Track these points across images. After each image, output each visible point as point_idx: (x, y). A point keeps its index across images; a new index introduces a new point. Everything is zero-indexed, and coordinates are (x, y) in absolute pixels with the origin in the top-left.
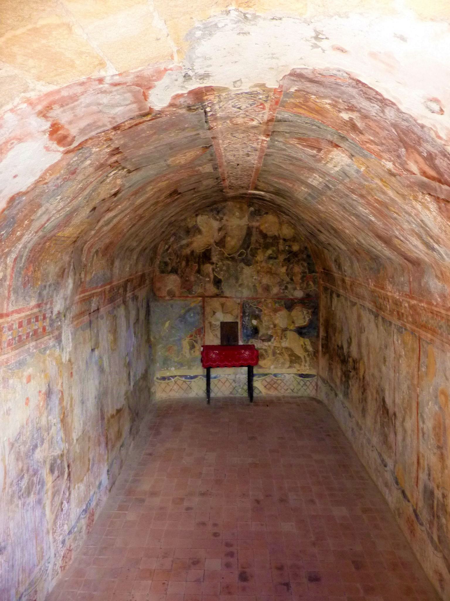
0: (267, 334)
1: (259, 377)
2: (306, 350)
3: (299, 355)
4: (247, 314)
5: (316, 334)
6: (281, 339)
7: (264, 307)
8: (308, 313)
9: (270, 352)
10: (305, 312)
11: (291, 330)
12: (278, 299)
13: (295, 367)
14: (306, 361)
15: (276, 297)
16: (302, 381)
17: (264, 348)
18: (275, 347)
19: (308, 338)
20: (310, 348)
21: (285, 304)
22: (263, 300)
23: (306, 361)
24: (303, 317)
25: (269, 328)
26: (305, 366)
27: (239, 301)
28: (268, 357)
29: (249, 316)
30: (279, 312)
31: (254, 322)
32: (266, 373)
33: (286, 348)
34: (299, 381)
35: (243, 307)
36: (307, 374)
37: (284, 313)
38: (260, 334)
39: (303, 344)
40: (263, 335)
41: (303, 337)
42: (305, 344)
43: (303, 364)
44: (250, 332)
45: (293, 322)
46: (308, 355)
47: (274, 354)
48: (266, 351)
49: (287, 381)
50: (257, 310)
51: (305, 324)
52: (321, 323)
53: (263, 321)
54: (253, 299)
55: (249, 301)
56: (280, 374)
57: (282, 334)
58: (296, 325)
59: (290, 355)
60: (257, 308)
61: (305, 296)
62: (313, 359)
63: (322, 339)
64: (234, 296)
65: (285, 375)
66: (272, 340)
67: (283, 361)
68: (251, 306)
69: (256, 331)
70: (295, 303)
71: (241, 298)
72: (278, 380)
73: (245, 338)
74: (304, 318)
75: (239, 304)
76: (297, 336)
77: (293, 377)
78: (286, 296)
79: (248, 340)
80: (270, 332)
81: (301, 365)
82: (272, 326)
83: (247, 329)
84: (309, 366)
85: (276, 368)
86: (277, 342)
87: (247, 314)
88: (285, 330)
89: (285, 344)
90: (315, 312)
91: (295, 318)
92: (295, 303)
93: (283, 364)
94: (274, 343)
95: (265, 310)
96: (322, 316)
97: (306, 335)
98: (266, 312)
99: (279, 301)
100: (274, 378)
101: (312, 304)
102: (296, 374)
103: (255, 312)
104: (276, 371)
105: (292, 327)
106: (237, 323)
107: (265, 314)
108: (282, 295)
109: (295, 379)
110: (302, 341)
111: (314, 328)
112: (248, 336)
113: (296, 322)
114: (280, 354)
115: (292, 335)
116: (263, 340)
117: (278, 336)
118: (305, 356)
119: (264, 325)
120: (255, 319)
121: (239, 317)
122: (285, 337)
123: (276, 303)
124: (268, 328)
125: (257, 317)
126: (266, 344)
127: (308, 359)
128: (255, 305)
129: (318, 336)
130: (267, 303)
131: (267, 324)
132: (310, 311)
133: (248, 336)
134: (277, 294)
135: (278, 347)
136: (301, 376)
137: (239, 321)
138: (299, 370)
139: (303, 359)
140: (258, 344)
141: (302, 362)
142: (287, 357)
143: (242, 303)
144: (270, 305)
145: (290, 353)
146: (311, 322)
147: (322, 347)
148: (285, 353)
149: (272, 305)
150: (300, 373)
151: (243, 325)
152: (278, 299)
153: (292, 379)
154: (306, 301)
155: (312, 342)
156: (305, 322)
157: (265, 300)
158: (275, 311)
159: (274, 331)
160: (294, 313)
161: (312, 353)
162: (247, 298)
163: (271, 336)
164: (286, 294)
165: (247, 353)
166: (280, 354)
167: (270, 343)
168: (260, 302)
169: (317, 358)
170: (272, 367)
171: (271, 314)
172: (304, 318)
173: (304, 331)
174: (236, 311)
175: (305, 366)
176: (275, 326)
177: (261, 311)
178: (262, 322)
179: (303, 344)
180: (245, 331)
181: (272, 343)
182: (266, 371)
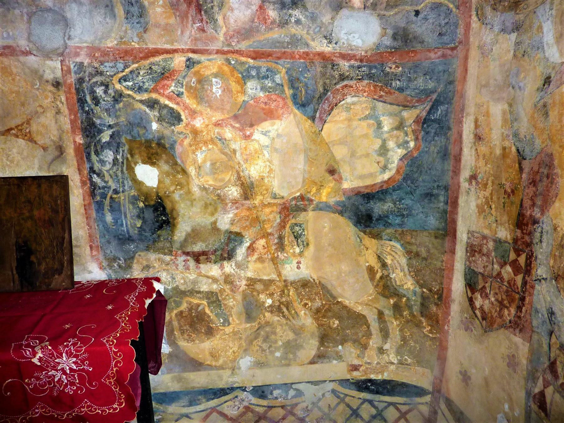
0: (215, 228)
1: (191, 404)
2: (386, 288)
3: (359, 309)
4: (105, 137)
5: (433, 221)
6: (281, 246)
7: (187, 99)
8: (400, 126)
9: (234, 303)
10: (387, 124)
11: (322, 208)
12: (257, 55)
13: (339, 357)
14: (385, 334)
15: (243, 46)
16: (366, 405)
17: (204, 288)
18: (252, 282)
19: (400, 237)
20: (406, 283)
21: (293, 82)
22: (179, 61)
23: (385, 334)
24: (378, 143)
25: (221, 199)
26: (381, 351)
27: (53, 68)
28: (227, 322)
29: (115, 143)
30: (266, 125)
31: (148, 175)
32: (221, 385)
33: (305, 284)
34: (355, 404)
35: (82, 101)
36: (385, 382)
37: (287, 126)
38: (182, 229)
39: (377, 266)
40: (195, 234)
41: (377, 236)
42: (384, 265)
43: (375, 341)
44: (131, 222)
45: (332, 172)
46: (397, 308)
47: (251, 310)
48: (214, 299)
49: (306, 409)
50: (153, 114)
51: (386, 176)
52: (465, 174)
53: (192, 171)
54: (126, 54)
55: (107, 68)
56: (276, 387)
57: (282, 226)
58: (346, 185)
59: (318, 313)
60: (152, 104)
61: (388, 41)
62: (419, 325)
63: (473, 250)
64: (23, 43)
65: (301, 387)
66: (241, 252)
67: (291, 336)
68: (118, 97)
69: (159, 214)
70: (343, 78)
71: (62, 54)
72: (270, 407)
73: (112, 249)
74: (383, 150)
75: (57, 84)
76: (348, 229)
77: (333, 391)
78: (295, 41)
79: (129, 259)
80: (225, 221)
81: (365, 347)
82: (234, 192)
83: (115, 207)
84: (398, 352)
85: (259, 364)
86: (260, 260)
87: (105, 137)
88: (292, 208)
89: (296, 267)
90: (437, 121)
91: (340, 152)
92: (343, 78)
93: (291, 348)
94: (246, 266)
95: (193, 113)
96: (478, 138)
97: (388, 225)
98: (198, 123)
99: (263, 64)
100: (254, 400)
101: (420, 82)
102: (344, 382)
103: (141, 123)
104: (262, 378)
105: (326, 195)
106: (62, 181)
107: (195, 132)
108: (276, 34)
109: (342, 400)
110: (370, 251)
111: (429, 196)
112: (124, 240)
113: (345, 170)
114: (276, 309)
115: (325, 227)
116: (198, 257)
117: (266, 235)
118: (381, 314)
119: (195, 189)
120: (151, 160)
121: (70, 151)
122: (297, 237)
123: (246, 77)
124: (217, 201)
125: (156, 150)
126: (214, 270)
127: (394, 325)
128: (140, 89)
129: (448, 231)
130: (202, 80)
131: (209, 181)
132: (409, 115)
133: (124, 240)
134: (246, 33)
135: (268, 284)
136: (364, 385)
137: (70, 170)
138: (355, 368)
139: (374, 326)
140: (169, 274)
141: (369, 335)
142: (306, 320)
143: (72, 79)
144: (216, 89)
145: (318, 303)
146: (413, 165)
147: (471, 285)
148: (298, 305)
149: (227, 90)
150: (357, 375)
151: (93, 190)
152: (257, 55)
153: (331, 400)
154: (391, 68)
155: (412, 255)
156: (385, 168)
157: (190, 64)
158: (247, 118)
159: (245, 213)
160: (335, 127)
161: (416, 302)
162: (92, 50)
163: (234, 238)
164: (294, 30)
165: (67, 363)
166: (276, 309)
167: (229, 267)
168: (165, 75)
169: (437, 323)
170: (245, 362)
171: (228, 134)
172: (383, 150)
173: (379, 208)
174: (48, 119)
175: (381, 351)
176: (248, 189)
177: (176, 118)
178: (184, 172)
179: (373, 261)
180: (109, 218)
181: (238, 266)
182: (225, 379)
